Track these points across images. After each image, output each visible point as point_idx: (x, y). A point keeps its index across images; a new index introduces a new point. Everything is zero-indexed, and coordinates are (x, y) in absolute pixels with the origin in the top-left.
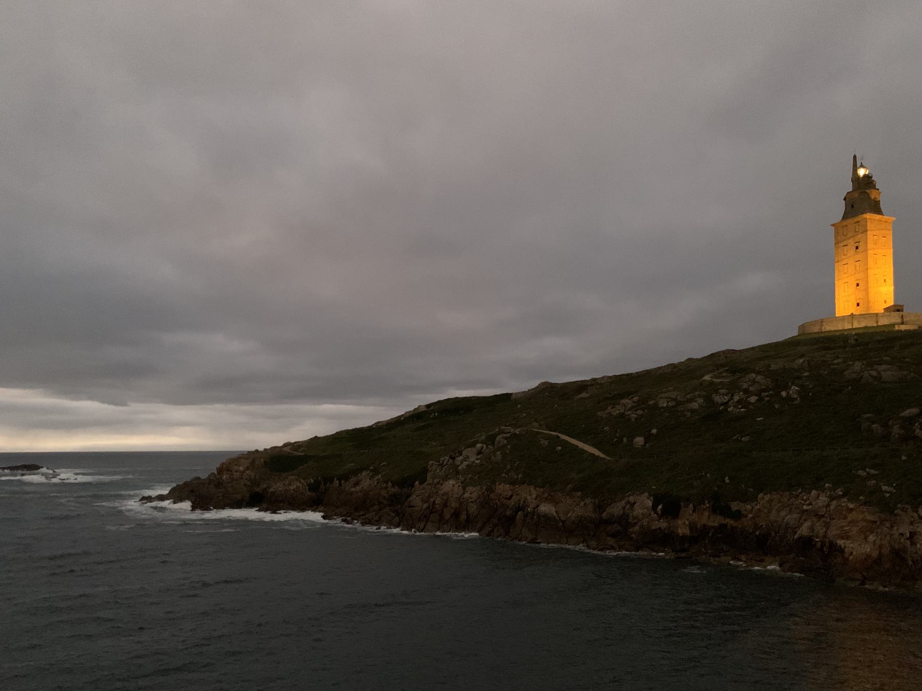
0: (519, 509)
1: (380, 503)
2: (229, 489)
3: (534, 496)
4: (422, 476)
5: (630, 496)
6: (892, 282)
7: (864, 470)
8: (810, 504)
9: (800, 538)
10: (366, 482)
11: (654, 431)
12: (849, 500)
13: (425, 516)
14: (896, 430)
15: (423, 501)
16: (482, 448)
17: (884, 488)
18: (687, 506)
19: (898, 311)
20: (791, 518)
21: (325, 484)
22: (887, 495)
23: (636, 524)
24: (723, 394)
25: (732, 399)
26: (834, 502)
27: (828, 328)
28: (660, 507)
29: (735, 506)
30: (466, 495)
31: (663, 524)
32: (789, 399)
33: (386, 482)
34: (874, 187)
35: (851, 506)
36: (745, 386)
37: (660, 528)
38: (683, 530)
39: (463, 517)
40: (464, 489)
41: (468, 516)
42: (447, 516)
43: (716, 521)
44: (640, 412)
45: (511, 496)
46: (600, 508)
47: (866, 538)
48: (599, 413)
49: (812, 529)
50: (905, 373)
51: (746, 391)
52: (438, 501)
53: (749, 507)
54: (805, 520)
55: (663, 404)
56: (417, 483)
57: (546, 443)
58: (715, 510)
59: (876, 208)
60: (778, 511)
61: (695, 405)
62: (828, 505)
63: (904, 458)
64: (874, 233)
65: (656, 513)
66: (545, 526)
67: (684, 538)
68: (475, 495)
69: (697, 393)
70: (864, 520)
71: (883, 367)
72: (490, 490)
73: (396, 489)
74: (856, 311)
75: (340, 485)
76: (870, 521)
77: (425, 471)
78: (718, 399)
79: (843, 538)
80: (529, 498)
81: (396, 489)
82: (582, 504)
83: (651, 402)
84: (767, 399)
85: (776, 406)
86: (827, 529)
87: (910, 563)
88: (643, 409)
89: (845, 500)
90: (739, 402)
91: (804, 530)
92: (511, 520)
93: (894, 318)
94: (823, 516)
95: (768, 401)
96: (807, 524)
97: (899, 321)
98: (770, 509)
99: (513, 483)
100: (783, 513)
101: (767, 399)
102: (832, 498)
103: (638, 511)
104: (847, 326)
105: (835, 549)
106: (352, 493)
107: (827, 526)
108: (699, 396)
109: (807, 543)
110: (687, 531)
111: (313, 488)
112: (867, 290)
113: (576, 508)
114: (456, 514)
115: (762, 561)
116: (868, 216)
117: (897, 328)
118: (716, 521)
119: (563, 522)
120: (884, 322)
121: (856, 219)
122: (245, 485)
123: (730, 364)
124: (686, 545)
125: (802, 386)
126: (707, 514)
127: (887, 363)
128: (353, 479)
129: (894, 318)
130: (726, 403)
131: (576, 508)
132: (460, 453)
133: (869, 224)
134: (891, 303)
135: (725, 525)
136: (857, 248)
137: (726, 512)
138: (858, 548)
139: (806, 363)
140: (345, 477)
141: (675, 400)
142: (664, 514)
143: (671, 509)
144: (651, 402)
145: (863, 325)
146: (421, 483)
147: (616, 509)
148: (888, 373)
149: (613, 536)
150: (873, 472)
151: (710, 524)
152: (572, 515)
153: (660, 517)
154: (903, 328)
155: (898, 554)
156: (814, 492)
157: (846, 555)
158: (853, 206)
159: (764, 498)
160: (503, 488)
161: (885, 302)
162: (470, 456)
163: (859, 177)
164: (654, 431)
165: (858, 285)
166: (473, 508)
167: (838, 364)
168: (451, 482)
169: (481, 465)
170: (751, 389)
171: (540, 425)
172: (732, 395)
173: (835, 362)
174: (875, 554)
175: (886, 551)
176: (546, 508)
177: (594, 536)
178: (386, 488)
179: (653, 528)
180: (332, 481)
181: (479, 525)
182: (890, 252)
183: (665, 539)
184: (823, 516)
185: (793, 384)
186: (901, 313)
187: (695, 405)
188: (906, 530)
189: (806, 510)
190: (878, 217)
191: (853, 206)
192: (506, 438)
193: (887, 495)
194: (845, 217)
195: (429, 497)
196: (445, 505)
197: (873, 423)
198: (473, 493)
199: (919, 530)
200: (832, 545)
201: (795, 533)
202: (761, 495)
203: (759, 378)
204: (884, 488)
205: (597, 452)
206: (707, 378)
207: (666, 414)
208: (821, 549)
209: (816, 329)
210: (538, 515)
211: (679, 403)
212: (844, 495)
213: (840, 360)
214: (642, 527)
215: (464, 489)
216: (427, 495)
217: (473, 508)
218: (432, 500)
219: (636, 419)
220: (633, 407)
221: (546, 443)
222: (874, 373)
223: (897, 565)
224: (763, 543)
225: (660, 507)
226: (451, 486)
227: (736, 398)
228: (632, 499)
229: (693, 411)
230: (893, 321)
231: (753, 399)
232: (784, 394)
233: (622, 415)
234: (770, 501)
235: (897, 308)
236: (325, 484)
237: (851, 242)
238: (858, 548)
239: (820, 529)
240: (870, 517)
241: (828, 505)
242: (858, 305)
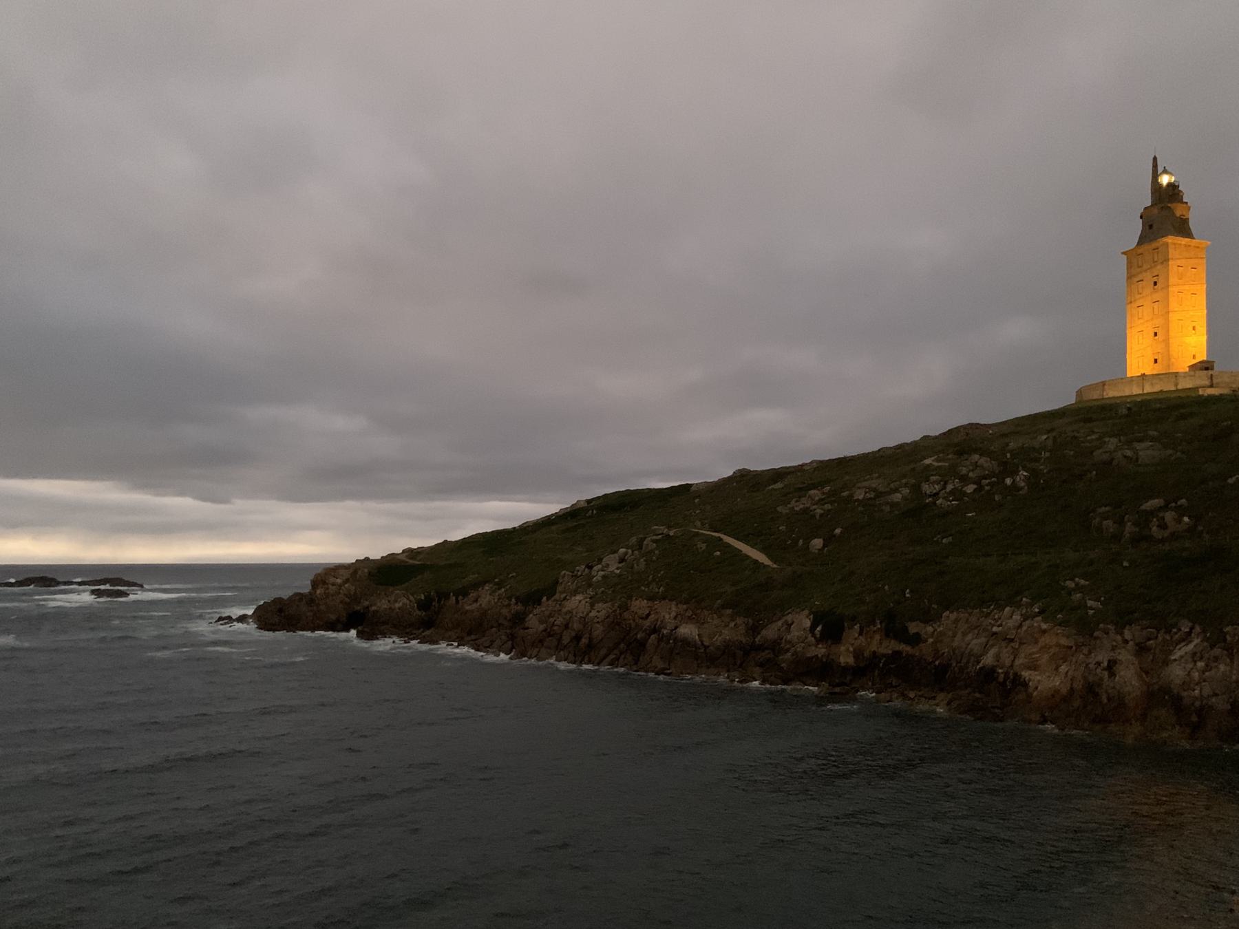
0: (655, 630)
1: (500, 625)
3: (673, 614)
6: (1204, 330)
7: (1072, 579)
8: (1000, 625)
9: (981, 669)
10: (486, 598)
12: (1045, 620)
14: (1129, 528)
15: (541, 622)
16: (626, 553)
17: (1090, 603)
18: (851, 627)
19: (1207, 369)
20: (976, 643)
21: (439, 601)
22: (1091, 612)
23: (788, 650)
24: (934, 482)
25: (944, 487)
26: (1028, 622)
27: (1111, 393)
29: (913, 628)
30: (593, 614)
33: (510, 598)
34: (1181, 201)
35: (1044, 626)
36: (964, 471)
38: (845, 657)
39: (584, 641)
40: (592, 605)
41: (590, 639)
42: (566, 639)
43: (888, 647)
44: (828, 507)
45: (649, 615)
46: (754, 630)
47: (1057, 669)
48: (779, 509)
49: (997, 657)
50: (1170, 452)
51: (964, 479)
53: (930, 629)
54: (992, 646)
55: (860, 495)
57: (704, 546)
59: (1183, 228)
60: (964, 634)
61: (897, 497)
62: (1020, 626)
63: (1126, 564)
64: (1179, 262)
67: (846, 669)
68: (603, 614)
69: (904, 481)
70: (1058, 645)
71: (1143, 445)
72: (625, 607)
73: (520, 607)
74: (1156, 369)
75: (457, 602)
76: (1064, 647)
77: (556, 583)
78: (926, 488)
79: (1029, 668)
80: (667, 616)
82: (732, 624)
83: (845, 494)
85: (997, 498)
87: (1105, 701)
89: (1039, 618)
90: (952, 492)
91: (988, 660)
92: (642, 645)
93: (1202, 379)
94: (1012, 640)
95: (988, 492)
96: (993, 651)
97: (1207, 383)
98: (957, 634)
100: (969, 637)
101: (987, 488)
103: (795, 633)
104: (1136, 391)
105: (1019, 683)
107: (1015, 654)
108: (906, 485)
109: (989, 674)
112: (1167, 341)
114: (577, 638)
115: (934, 698)
116: (1170, 239)
117: (1201, 392)
118: (888, 647)
119: (706, 647)
120: (1185, 384)
121: (1154, 245)
123: (963, 442)
124: (848, 678)
125: (1034, 473)
126: (877, 637)
127: (1153, 439)
128: (473, 595)
129: (1202, 379)
130: (937, 494)
131: (725, 630)
132: (600, 561)
133: (1171, 251)
134: (1202, 356)
136: (1155, 283)
138: (1046, 681)
139: (1050, 442)
140: (464, 592)
141: (874, 490)
144: (845, 494)
145: (1157, 389)
147: (770, 632)
148: (1147, 452)
149: (761, 665)
150: (1083, 582)
151: (882, 650)
152: (718, 640)
153: (818, 641)
154: (1210, 391)
155: (1091, 689)
156: (1008, 609)
157: (1030, 690)
158: (1151, 227)
159: (949, 616)
160: (639, 605)
161: (1194, 357)
162: (612, 564)
163: (1161, 185)
164: (838, 531)
165: (1156, 334)
166: (598, 631)
167: (1090, 442)
168: (579, 597)
169: (620, 576)
170: (971, 474)
171: (703, 524)
172: (946, 483)
174: (1064, 691)
175: (1078, 685)
176: (688, 630)
177: (741, 666)
178: (509, 605)
179: (809, 655)
180: (447, 597)
181: (603, 652)
182: (1202, 289)
183: (821, 670)
184: (1012, 640)
185: (1024, 468)
186: (1210, 372)
187: (897, 497)
188: (1103, 657)
189: (995, 633)
190: (1184, 241)
191: (1151, 227)
193: (1091, 612)
194: (1142, 240)
195: (550, 616)
196: (567, 626)
198: (601, 611)
199: (1120, 657)
201: (978, 662)
203: (983, 461)
204: (1090, 603)
206: (927, 461)
207: (860, 509)
208: (1003, 684)
209: (1095, 395)
210: (675, 639)
211: (879, 494)
214: (795, 653)
215: (592, 605)
216: (547, 613)
217: (598, 631)
218: (552, 620)
219: (821, 515)
221: (704, 546)
222: (1129, 453)
223: (1089, 704)
224: (940, 676)
226: (577, 603)
227: (950, 487)
228: (789, 618)
229: (894, 505)
230: (1199, 382)
231: (970, 489)
232: (1008, 481)
233: (806, 511)
234: (956, 621)
235: (1206, 366)
236: (439, 601)
237: (1148, 277)
238: (1046, 681)
240: (1064, 641)
241: (1020, 626)
242: (1156, 361)
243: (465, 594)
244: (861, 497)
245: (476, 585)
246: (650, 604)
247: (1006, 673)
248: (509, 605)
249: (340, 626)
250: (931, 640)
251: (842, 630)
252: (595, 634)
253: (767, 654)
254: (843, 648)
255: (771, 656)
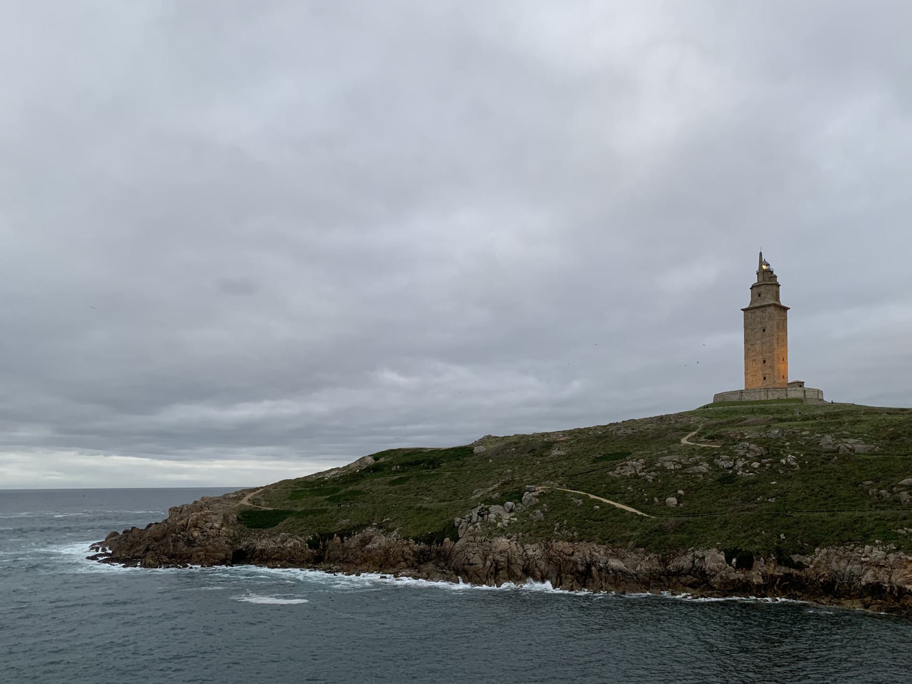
0: (588, 566)
1: (406, 560)
2: (210, 547)
3: (602, 552)
4: (452, 532)
5: (693, 551)
8: (866, 557)
11: (681, 492)
12: (906, 553)
13: (492, 573)
18: (759, 560)
20: (855, 568)
23: (714, 575)
28: (734, 560)
29: (796, 558)
31: (740, 575)
32: (788, 465)
37: (738, 579)
38: (757, 580)
45: (573, 553)
49: (874, 576)
52: (498, 557)
53: (809, 559)
54: (867, 569)
56: (447, 540)
57: (580, 501)
58: (779, 562)
62: (886, 558)
65: (731, 565)
66: (618, 579)
67: (759, 586)
73: (423, 546)
75: (342, 541)
81: (417, 547)
82: (647, 558)
83: (658, 465)
84: (768, 465)
86: (891, 576)
88: (655, 471)
91: (868, 577)
98: (823, 561)
99: (571, 540)
100: (843, 564)
102: (889, 553)
106: (369, 551)
107: (890, 574)
109: (875, 590)
110: (761, 581)
111: (313, 545)
113: (645, 563)
119: (636, 575)
122: (227, 542)
126: (773, 565)
128: (358, 537)
131: (645, 563)
135: (791, 574)
137: (789, 563)
139: (780, 434)
140: (345, 533)
142: (738, 567)
143: (746, 562)
146: (455, 539)
147: (685, 562)
151: (777, 574)
156: (867, 547)
159: (821, 553)
160: (561, 545)
173: (804, 433)
176: (615, 563)
180: (331, 537)
192: (537, 497)
197: (880, 489)
200: (901, 590)
201: (860, 580)
202: (817, 549)
205: (639, 513)
210: (612, 569)
211: (685, 467)
212: (898, 549)
213: (807, 433)
214: (721, 577)
216: (481, 552)
219: (653, 480)
220: (644, 469)
221: (580, 501)
225: (734, 560)
229: (704, 474)
233: (636, 476)
234: (827, 554)
236: (324, 541)
239: (883, 576)
243: (349, 535)
244: (673, 467)
245: (360, 527)
246: (571, 544)
247: (892, 588)
248: (408, 544)
249: (229, 562)
250: (812, 566)
251: (753, 562)
252: (542, 567)
253: (690, 579)
254: (753, 573)
255: (695, 579)
